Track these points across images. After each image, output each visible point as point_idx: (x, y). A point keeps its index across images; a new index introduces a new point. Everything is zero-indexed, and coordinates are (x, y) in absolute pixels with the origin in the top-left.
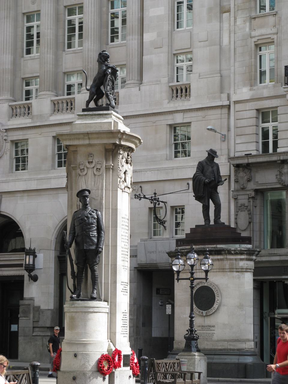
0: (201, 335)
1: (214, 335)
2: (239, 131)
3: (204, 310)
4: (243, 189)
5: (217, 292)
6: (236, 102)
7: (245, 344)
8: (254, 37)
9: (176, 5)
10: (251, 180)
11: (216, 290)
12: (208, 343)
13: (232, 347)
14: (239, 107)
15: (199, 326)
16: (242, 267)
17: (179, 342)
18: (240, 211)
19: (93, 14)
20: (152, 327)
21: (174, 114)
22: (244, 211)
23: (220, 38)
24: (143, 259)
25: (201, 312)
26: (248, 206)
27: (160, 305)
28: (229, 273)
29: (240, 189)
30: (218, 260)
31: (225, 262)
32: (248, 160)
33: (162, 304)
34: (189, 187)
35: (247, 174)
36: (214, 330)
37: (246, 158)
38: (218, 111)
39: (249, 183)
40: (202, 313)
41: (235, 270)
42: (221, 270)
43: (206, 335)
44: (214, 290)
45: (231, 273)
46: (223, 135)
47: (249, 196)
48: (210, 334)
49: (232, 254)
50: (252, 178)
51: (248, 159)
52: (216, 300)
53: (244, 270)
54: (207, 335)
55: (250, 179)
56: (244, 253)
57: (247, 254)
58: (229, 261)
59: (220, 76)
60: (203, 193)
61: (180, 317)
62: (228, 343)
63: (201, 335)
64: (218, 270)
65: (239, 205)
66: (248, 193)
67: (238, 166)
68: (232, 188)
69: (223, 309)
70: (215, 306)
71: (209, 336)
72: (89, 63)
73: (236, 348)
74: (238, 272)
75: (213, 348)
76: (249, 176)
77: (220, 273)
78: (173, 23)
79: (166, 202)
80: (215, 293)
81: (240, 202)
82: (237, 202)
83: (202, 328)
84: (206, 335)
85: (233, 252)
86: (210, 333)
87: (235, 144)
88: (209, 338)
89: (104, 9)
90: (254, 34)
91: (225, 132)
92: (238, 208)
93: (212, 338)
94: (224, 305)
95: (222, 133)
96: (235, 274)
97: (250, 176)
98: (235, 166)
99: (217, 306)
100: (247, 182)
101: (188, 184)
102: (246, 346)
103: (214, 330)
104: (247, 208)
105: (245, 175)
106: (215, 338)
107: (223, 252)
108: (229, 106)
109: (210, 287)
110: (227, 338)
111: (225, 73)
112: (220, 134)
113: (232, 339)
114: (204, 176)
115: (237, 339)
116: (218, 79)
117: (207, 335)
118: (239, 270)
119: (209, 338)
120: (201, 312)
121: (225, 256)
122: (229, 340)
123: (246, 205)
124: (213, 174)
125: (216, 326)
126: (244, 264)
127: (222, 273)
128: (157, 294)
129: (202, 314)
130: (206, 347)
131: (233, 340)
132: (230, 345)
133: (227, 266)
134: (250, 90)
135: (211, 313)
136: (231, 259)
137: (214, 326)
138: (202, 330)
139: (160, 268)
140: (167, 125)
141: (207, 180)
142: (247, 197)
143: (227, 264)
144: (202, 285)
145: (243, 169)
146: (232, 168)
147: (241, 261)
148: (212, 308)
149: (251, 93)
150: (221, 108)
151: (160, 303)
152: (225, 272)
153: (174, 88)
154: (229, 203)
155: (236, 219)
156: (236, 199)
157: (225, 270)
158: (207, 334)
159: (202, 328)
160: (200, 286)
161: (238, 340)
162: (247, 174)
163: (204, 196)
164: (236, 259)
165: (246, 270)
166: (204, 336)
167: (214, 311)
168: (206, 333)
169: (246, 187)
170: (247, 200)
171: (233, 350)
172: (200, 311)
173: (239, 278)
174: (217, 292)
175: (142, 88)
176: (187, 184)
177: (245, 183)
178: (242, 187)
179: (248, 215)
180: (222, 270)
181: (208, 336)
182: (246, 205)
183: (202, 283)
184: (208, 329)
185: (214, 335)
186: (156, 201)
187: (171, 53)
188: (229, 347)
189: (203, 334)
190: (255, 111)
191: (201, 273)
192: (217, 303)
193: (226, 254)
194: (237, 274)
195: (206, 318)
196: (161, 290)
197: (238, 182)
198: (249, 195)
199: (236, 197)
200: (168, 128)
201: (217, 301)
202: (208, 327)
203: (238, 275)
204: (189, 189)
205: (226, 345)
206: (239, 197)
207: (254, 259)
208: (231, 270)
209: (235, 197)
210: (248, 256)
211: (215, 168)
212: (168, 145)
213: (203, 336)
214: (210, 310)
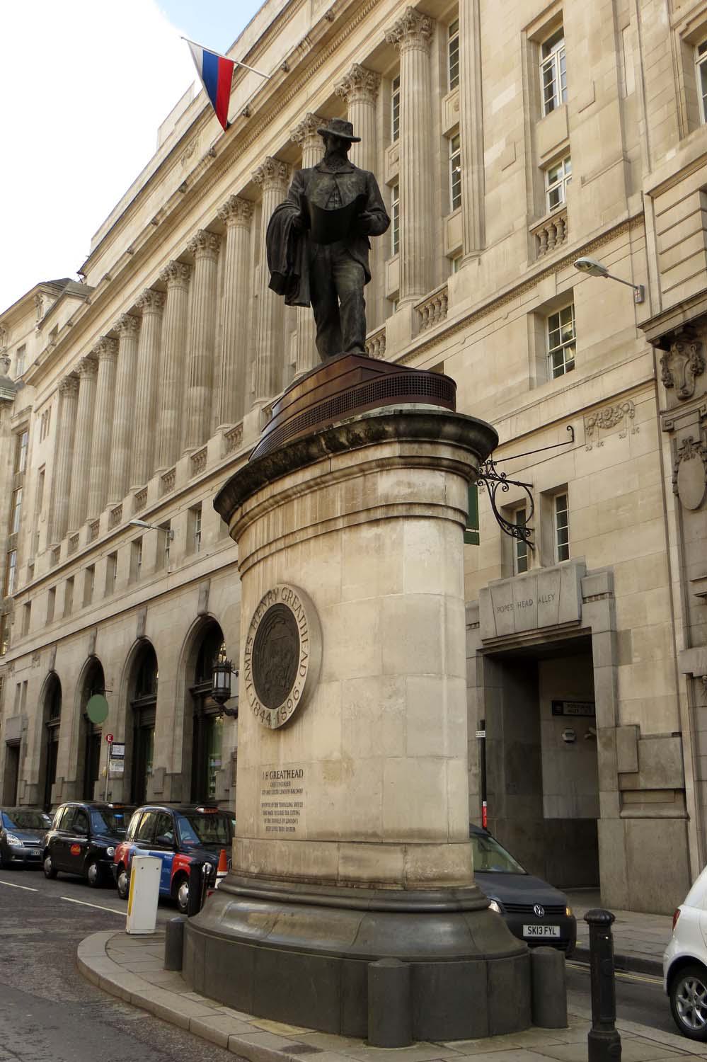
2: (667, 260)
4: (686, 398)
6: (654, 194)
7: (400, 856)
8: (679, 23)
9: (542, 72)
10: (703, 369)
13: (351, 871)
14: (662, 202)
16: (387, 497)
18: (683, 459)
19: (412, 164)
20: (541, 795)
21: (538, 284)
22: (693, 457)
23: (620, 81)
24: (489, 629)
26: (700, 442)
27: (567, 741)
29: (677, 400)
32: (684, 316)
33: (572, 739)
34: (573, 436)
35: (691, 357)
36: (300, 791)
37: (679, 311)
38: (624, 238)
39: (699, 380)
41: (363, 517)
42: (320, 530)
46: (636, 288)
47: (702, 414)
50: (704, 365)
51: (684, 312)
52: (301, 656)
55: (700, 365)
57: (400, 437)
59: (624, 160)
60: (291, 264)
62: (338, 849)
65: (680, 445)
66: (698, 406)
67: (664, 342)
68: (664, 407)
70: (300, 683)
72: (407, 255)
73: (365, 873)
74: (376, 522)
76: (696, 359)
77: (322, 542)
78: (534, 107)
79: (531, 486)
81: (681, 435)
82: (675, 439)
83: (272, 781)
85: (343, 440)
87: (661, 293)
89: (438, 156)
90: (676, 16)
91: (641, 281)
92: (680, 452)
95: (636, 285)
96: (368, 533)
97: (698, 359)
98: (658, 343)
100: (693, 378)
101: (570, 428)
102: (408, 866)
103: (300, 791)
104: (697, 448)
105: (687, 360)
107: (314, 450)
108: (642, 214)
110: (338, 827)
111: (632, 153)
112: (631, 288)
115: (370, 831)
116: (618, 170)
118: (379, 514)
122: (344, 835)
123: (697, 439)
124: (337, 199)
125: (306, 773)
126: (399, 483)
128: (553, 714)
131: (357, 834)
132: (346, 859)
134: (681, 148)
135: (289, 715)
137: (299, 774)
139: (525, 645)
140: (528, 313)
142: (695, 417)
143: (337, 499)
144: (272, 603)
145: (680, 347)
146: (660, 353)
147: (385, 472)
148: (291, 696)
149: (685, 151)
150: (630, 230)
151: (564, 735)
152: (334, 533)
153: (540, 232)
154: (661, 449)
155: (675, 483)
156: (671, 431)
157: (332, 526)
161: (375, 835)
162: (691, 357)
163: (297, 273)
164: (363, 469)
165: (411, 510)
167: (295, 704)
169: (692, 392)
170: (697, 424)
173: (379, 549)
175: (485, 257)
176: (568, 430)
177: (688, 382)
178: (681, 394)
179: (703, 464)
182: (694, 442)
185: (302, 811)
186: (497, 480)
187: (534, 167)
190: (699, 192)
196: (565, 705)
197: (672, 385)
198: (700, 411)
199: (671, 427)
200: (532, 317)
203: (378, 537)
204: (573, 441)
206: (678, 425)
207: (445, 463)
209: (667, 428)
210: (406, 446)
211: (348, 181)
212: (534, 358)
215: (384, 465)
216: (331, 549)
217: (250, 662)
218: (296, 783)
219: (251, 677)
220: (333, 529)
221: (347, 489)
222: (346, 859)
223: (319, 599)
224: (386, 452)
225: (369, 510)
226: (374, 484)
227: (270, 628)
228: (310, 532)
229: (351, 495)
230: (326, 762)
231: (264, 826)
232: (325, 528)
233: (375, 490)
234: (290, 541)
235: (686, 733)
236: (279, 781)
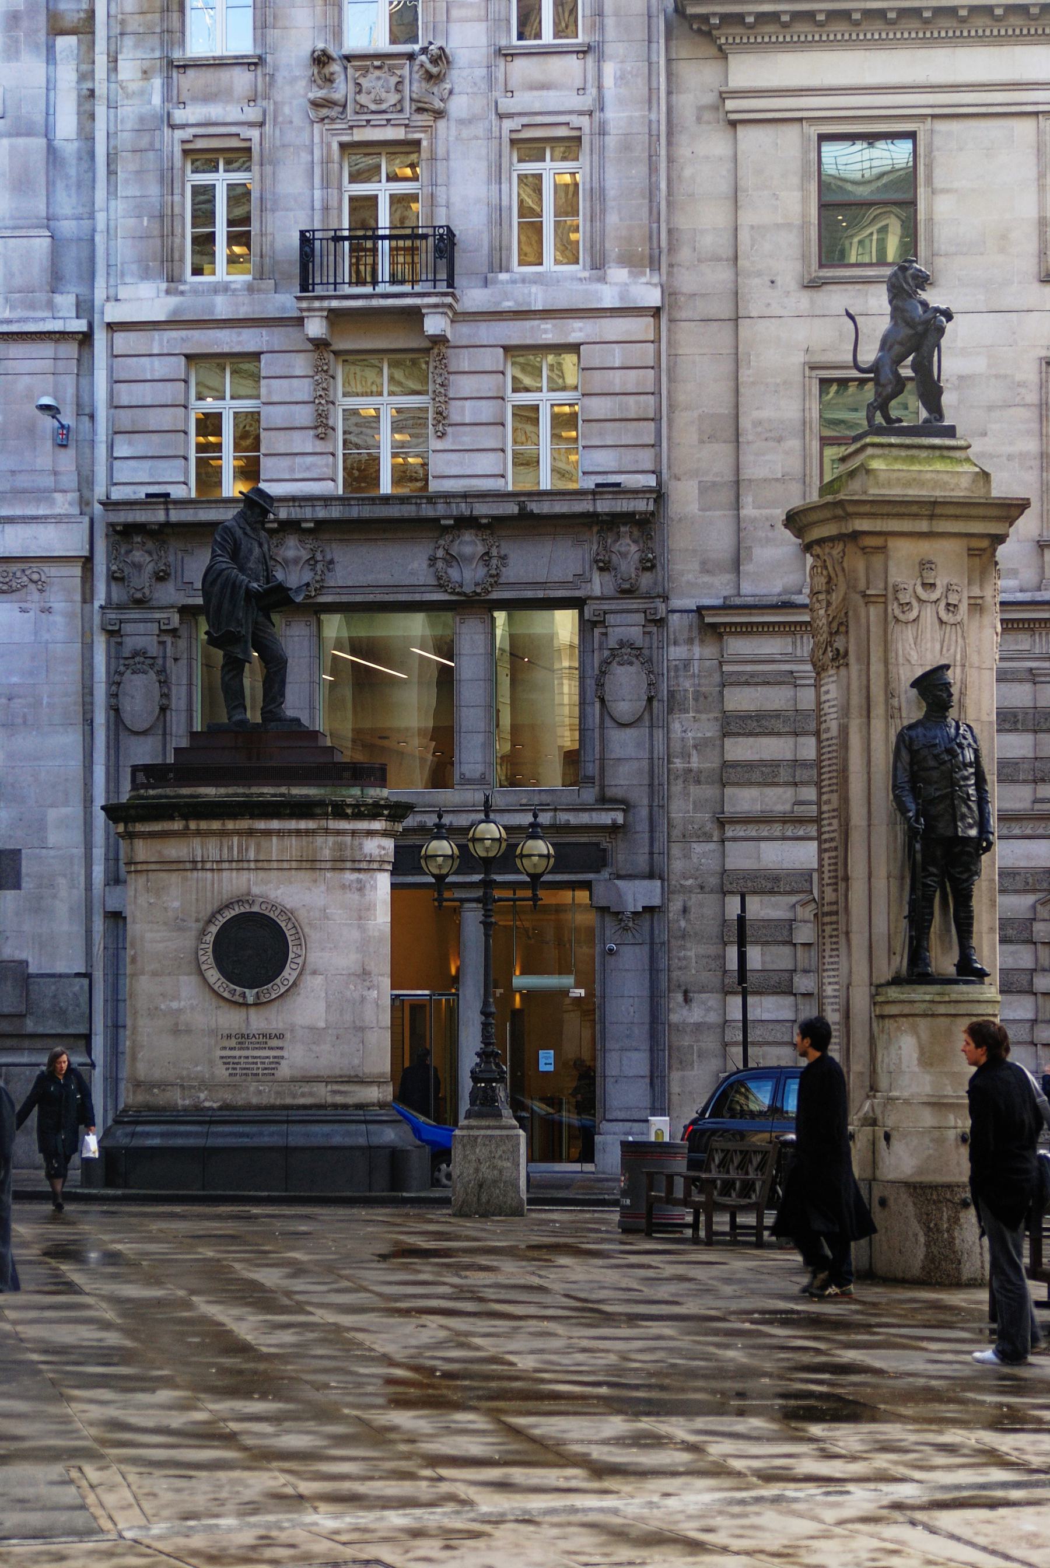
1: (283, 1062)
3: (251, 987)
5: (293, 931)
11: (290, 926)
13: (339, 1099)
15: (229, 1036)
17: (154, 1086)
28: (329, 875)
30: (298, 832)
31: (319, 840)
36: (281, 1048)
40: (244, 995)
41: (349, 865)
42: (304, 865)
44: (283, 925)
45: (337, 875)
49: (344, 816)
52: (291, 955)
53: (375, 866)
56: (382, 815)
58: (331, 840)
61: (156, 1008)
64: (294, 865)
69: (313, 983)
70: (289, 974)
73: (350, 1100)
74: (359, 870)
75: (278, 1102)
77: (302, 874)
80: (288, 934)
85: (349, 811)
94: (314, 973)
96: (350, 877)
99: (295, 974)
103: (281, 1048)
106: (284, 1070)
107: (318, 811)
109: (271, 915)
113: (338, 1072)
114: (242, 569)
118: (364, 865)
121: (323, 823)
125: (288, 1035)
127: (309, 872)
129: (241, 1000)
130: (255, 1100)
132: (334, 1092)
133: (327, 854)
136: (339, 832)
137: (280, 1036)
138: (241, 1049)
141: (255, 585)
143: (325, 847)
144: (243, 910)
148: (278, 981)
160: (233, 913)
161: (357, 1076)
164: (354, 833)
171: (345, 1107)
173: (361, 890)
174: (293, 931)
185: (283, 1062)
188: (330, 1100)
189: (242, 1060)
191: (234, 873)
192: (294, 966)
193: (325, 816)
194: (356, 876)
195: (252, 1011)
205: (323, 1093)
208: (339, 864)
215: (370, 833)
216: (315, 881)
217: (210, 950)
218: (275, 1043)
219: (211, 960)
221: (335, 843)
222: (334, 1092)
223: (302, 915)
224: (377, 825)
225: (354, 861)
226: (361, 844)
228: (294, 865)
229: (341, 847)
230: (312, 1029)
231: (227, 1073)
232: (310, 864)
233: (361, 849)
234: (260, 865)
235: (98, 975)
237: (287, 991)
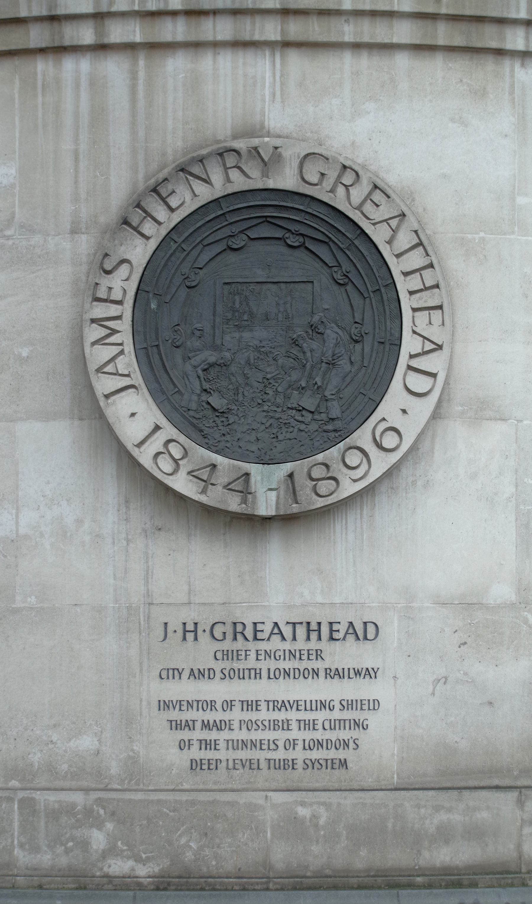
0: (219, 726)
12: (303, 812)
25: (221, 478)
43: (275, 725)
48: (321, 716)
54: (286, 725)
63: (219, 726)
71: (308, 735)
83: (227, 645)
84: (275, 725)
86: (323, 705)
88: (315, 755)
93: (341, 754)
117: (286, 725)
119: (315, 755)
120: (221, 478)
158: (293, 715)
159: (227, 645)
166: (256, 735)
168: (284, 705)
172: (214, 466)
180: (463, 26)
181: (295, 734)
183: (231, 160)
184: (305, 664)
201: (419, 363)
202: (301, 644)
213: (244, 735)
214: (334, 452)
220: (494, 45)
227: (222, 246)
236: (263, 646)
237: (389, 474)
